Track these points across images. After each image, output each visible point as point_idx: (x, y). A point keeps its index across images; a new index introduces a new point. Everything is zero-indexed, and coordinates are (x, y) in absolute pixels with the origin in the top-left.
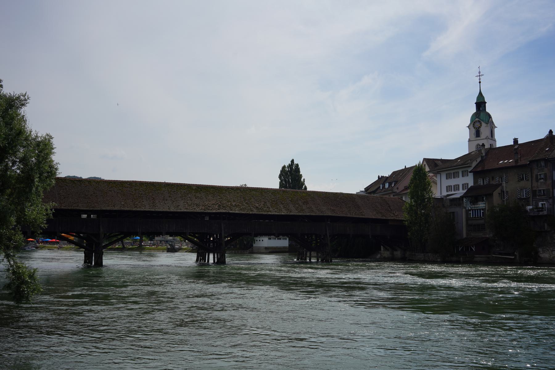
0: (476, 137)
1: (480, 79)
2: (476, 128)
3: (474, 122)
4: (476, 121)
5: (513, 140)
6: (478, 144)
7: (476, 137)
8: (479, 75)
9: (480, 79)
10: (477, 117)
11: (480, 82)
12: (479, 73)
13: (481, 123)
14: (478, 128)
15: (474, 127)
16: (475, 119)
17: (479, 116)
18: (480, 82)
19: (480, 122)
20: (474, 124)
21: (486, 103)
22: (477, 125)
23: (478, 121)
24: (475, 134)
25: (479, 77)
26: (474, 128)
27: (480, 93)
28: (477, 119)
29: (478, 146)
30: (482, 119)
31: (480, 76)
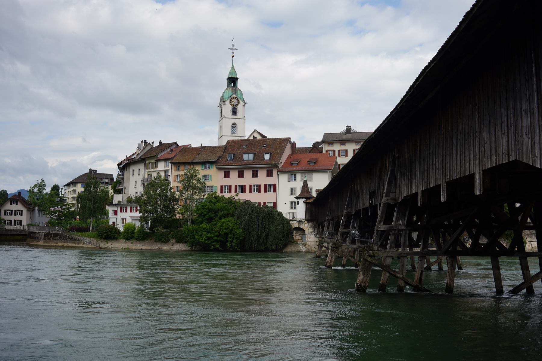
0: (233, 115)
1: (233, 53)
2: (232, 105)
3: (232, 99)
4: (233, 97)
5: (346, 128)
6: (234, 123)
7: (233, 115)
8: (232, 48)
9: (233, 53)
10: (234, 94)
11: (233, 57)
12: (233, 46)
13: (239, 101)
14: (235, 105)
15: (231, 103)
16: (232, 95)
17: (236, 92)
18: (233, 57)
19: (237, 99)
20: (230, 100)
21: (237, 79)
22: (234, 102)
23: (236, 98)
24: (232, 111)
25: (232, 50)
26: (231, 105)
27: (233, 68)
28: (234, 96)
29: (233, 125)
30: (238, 96)
31: (234, 50)
